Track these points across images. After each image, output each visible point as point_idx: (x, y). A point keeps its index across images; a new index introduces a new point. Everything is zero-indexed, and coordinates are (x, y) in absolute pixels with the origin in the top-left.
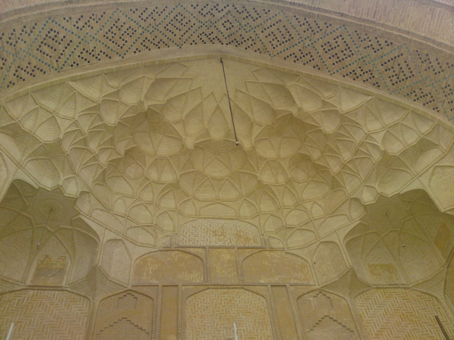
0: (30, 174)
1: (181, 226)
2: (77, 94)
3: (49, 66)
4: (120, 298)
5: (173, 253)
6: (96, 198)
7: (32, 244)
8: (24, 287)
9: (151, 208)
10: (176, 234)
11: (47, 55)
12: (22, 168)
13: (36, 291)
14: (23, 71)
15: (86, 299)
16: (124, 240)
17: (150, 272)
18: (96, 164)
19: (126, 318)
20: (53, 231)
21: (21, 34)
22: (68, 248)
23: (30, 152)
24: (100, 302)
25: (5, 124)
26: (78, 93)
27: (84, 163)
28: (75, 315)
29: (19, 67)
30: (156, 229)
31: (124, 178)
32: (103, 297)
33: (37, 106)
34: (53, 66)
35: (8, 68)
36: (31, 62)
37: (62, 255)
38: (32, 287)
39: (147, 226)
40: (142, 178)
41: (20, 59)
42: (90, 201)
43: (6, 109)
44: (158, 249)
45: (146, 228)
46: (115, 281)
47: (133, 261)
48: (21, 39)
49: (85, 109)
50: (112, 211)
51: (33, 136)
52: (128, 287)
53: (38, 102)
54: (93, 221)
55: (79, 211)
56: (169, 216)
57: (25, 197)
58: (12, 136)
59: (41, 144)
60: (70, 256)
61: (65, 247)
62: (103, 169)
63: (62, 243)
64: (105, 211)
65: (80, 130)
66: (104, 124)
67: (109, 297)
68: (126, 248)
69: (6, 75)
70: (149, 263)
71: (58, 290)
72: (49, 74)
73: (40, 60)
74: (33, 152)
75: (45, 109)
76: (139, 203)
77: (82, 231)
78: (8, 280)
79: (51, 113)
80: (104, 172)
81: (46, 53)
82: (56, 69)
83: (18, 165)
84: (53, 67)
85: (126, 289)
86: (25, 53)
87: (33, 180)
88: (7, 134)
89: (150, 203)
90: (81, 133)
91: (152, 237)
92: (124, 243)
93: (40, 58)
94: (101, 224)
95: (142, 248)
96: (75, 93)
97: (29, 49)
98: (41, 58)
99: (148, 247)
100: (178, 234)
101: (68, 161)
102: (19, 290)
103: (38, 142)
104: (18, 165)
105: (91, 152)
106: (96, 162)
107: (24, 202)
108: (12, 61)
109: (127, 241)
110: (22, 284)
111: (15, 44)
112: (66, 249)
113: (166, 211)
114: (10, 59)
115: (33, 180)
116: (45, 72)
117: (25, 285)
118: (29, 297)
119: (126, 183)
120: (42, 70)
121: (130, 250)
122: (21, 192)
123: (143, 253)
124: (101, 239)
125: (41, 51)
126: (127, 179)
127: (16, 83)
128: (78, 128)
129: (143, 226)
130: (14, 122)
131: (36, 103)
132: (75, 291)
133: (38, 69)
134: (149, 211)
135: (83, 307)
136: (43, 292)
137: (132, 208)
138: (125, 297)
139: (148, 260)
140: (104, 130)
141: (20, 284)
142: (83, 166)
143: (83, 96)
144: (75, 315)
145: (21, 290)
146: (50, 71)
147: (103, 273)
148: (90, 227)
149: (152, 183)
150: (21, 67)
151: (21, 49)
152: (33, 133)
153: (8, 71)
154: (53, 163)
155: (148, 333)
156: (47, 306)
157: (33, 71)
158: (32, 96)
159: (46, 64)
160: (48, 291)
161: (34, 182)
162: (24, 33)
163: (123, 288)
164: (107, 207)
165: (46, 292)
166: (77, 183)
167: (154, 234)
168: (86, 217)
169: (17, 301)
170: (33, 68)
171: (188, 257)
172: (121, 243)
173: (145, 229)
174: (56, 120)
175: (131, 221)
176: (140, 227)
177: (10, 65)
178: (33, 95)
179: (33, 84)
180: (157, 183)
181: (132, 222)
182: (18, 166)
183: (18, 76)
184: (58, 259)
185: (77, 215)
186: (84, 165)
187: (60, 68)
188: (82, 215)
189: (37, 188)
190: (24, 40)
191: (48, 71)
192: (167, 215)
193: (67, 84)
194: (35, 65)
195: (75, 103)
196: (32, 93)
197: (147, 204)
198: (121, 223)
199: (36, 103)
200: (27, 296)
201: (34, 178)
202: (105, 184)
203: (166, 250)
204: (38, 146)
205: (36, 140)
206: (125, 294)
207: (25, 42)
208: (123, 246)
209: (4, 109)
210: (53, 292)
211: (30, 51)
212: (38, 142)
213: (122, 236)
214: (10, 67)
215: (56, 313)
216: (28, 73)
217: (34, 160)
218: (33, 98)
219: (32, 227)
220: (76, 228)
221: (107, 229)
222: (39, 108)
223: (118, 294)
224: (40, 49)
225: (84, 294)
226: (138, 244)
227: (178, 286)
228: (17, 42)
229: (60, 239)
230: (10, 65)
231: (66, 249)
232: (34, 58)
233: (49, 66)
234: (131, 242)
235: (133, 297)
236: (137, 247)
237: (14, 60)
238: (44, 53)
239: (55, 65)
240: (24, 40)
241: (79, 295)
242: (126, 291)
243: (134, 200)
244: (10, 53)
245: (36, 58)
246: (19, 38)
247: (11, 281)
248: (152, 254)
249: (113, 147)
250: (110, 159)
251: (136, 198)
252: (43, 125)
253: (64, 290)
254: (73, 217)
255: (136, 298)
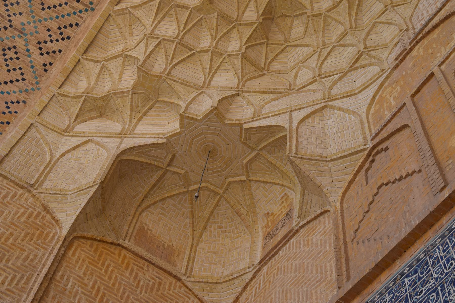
0: (143, 134)
1: (411, 18)
2: (133, 11)
3: (75, 13)
4: (368, 169)
5: (414, 53)
6: (255, 92)
7: (240, 216)
8: (255, 270)
9: (349, 39)
10: (407, 30)
11: (60, 5)
12: (128, 136)
13: (270, 263)
14: (49, 43)
15: (326, 215)
16: (331, 103)
17: (393, 103)
18: (225, 58)
19: (383, 183)
20: (244, 178)
21: (7, 10)
22: (280, 182)
23: (129, 113)
24: (342, 200)
25: (78, 109)
26: (133, 7)
27: (207, 71)
28: (319, 244)
29: (39, 43)
30: (372, 52)
31: (291, 46)
32: (342, 190)
33: (102, 64)
34: (78, 10)
35: (27, 53)
36: (49, 28)
37: (281, 196)
38: (263, 262)
39: (356, 62)
40: (310, 22)
41: (31, 34)
42: (249, 102)
43: (64, 94)
44: (390, 70)
45: (357, 65)
46: (340, 155)
47: (364, 116)
48: (12, 14)
49: (154, 15)
50: (294, 89)
51: (115, 94)
52: (368, 146)
53: (100, 59)
54: (266, 117)
55: (237, 122)
56: (383, 23)
57: (169, 165)
58: (101, 116)
59: (130, 93)
60: (289, 188)
61: (275, 184)
62: (240, 56)
63: (267, 182)
64: (281, 97)
65: (163, 39)
66: (194, 8)
67: (351, 182)
68: (340, 109)
69: (31, 62)
70: (388, 97)
71: (292, 237)
72: (84, 22)
73: (57, 17)
74: (132, 110)
75: (112, 58)
76: (329, 49)
77: (267, 142)
78: (231, 277)
79: (121, 55)
80: (244, 57)
81: (57, 5)
82: (86, 10)
83: (120, 136)
84: (81, 12)
85: (366, 152)
86: (32, 24)
87: (153, 138)
88: (92, 118)
89: (344, 35)
90: (169, 41)
91: (375, 67)
92: (332, 107)
93: (55, 15)
94: (281, 112)
95: (367, 90)
96: (130, 12)
97: (33, 17)
98: (56, 15)
99: (374, 81)
100: (411, 26)
101: (174, 81)
102: (251, 280)
103: (125, 94)
104: (120, 136)
105: (204, 51)
106: (224, 56)
107: (176, 173)
108: (23, 43)
109: (336, 101)
110: (251, 269)
111: (9, 24)
112: (278, 184)
113: (377, 22)
114: (20, 43)
115: (153, 138)
116: (77, 24)
117: (254, 266)
118: (264, 276)
119: (299, 49)
120: (71, 26)
121: (350, 108)
122: (155, 163)
123: (372, 94)
124: (287, 126)
125: (49, 8)
126: (296, 43)
127: (52, 61)
128: (159, 40)
129: (351, 66)
130: (83, 98)
131: (97, 62)
132: (308, 219)
133: (65, 27)
134: (349, 45)
135: (326, 226)
136: (276, 256)
137: (322, 63)
138: (373, 165)
139: (385, 94)
140: (202, 15)
141: (248, 270)
142: (211, 74)
143: (140, 5)
144: (319, 244)
145: (254, 276)
146: (82, 18)
147: (309, 159)
148: (267, 127)
149: (329, 14)
150: (42, 41)
151: (23, 24)
152: (113, 90)
153: (30, 56)
154: (165, 102)
155: (420, 171)
156: (284, 267)
157: (61, 34)
158: (86, 59)
159: (69, 15)
160: (282, 250)
161: (155, 138)
162: (10, 6)
163: (362, 153)
164: (283, 91)
165: (280, 252)
166: (209, 96)
167: (373, 60)
168: (253, 121)
169: (253, 293)
170: (59, 31)
171: (437, 31)
172: (328, 110)
173: (356, 68)
174: (130, 56)
175: (330, 76)
176: (349, 71)
177: (25, 48)
178: (86, 57)
179: (75, 46)
180: (335, 7)
181: (331, 77)
182: (121, 137)
183: (48, 53)
184: (280, 205)
185: (241, 129)
186: (210, 72)
187: (90, 5)
188: (245, 123)
189: (164, 141)
190: (17, 13)
191: (79, 19)
192: (381, 25)
193: (115, 12)
194: (57, 25)
195: (140, 21)
196: (84, 57)
197: (340, 40)
198: (314, 91)
199: (97, 62)
200: (262, 277)
201: (151, 134)
202: (266, 72)
203: (402, 61)
204: (129, 99)
205: (122, 94)
206: (371, 158)
207: (21, 14)
208: (337, 112)
209: (62, 95)
210: (288, 245)
211: (37, 18)
212: (125, 94)
213: (322, 101)
214: (28, 50)
215: (296, 265)
216: (57, 40)
217: (141, 118)
218: (90, 60)
219: (219, 196)
220: (260, 147)
221: (294, 110)
222: (105, 63)
223: (361, 168)
224: (46, 6)
225: (319, 212)
226: (357, 92)
227: (432, 75)
228: (10, 21)
229: (261, 179)
230: (25, 48)
231: (278, 184)
232: (49, 20)
233: (75, 13)
234: (343, 97)
235: (383, 152)
236: (359, 95)
237: (26, 40)
238: (55, 7)
239: (80, 6)
240: (17, 13)
241: (316, 218)
242: (369, 155)
243: (317, 53)
244: (14, 37)
245: (51, 19)
246: (9, 16)
247: (235, 276)
248: (386, 84)
249: (234, 24)
250: (244, 41)
251: (319, 49)
252: (124, 75)
253: (297, 231)
254: (241, 136)
255: (387, 149)
